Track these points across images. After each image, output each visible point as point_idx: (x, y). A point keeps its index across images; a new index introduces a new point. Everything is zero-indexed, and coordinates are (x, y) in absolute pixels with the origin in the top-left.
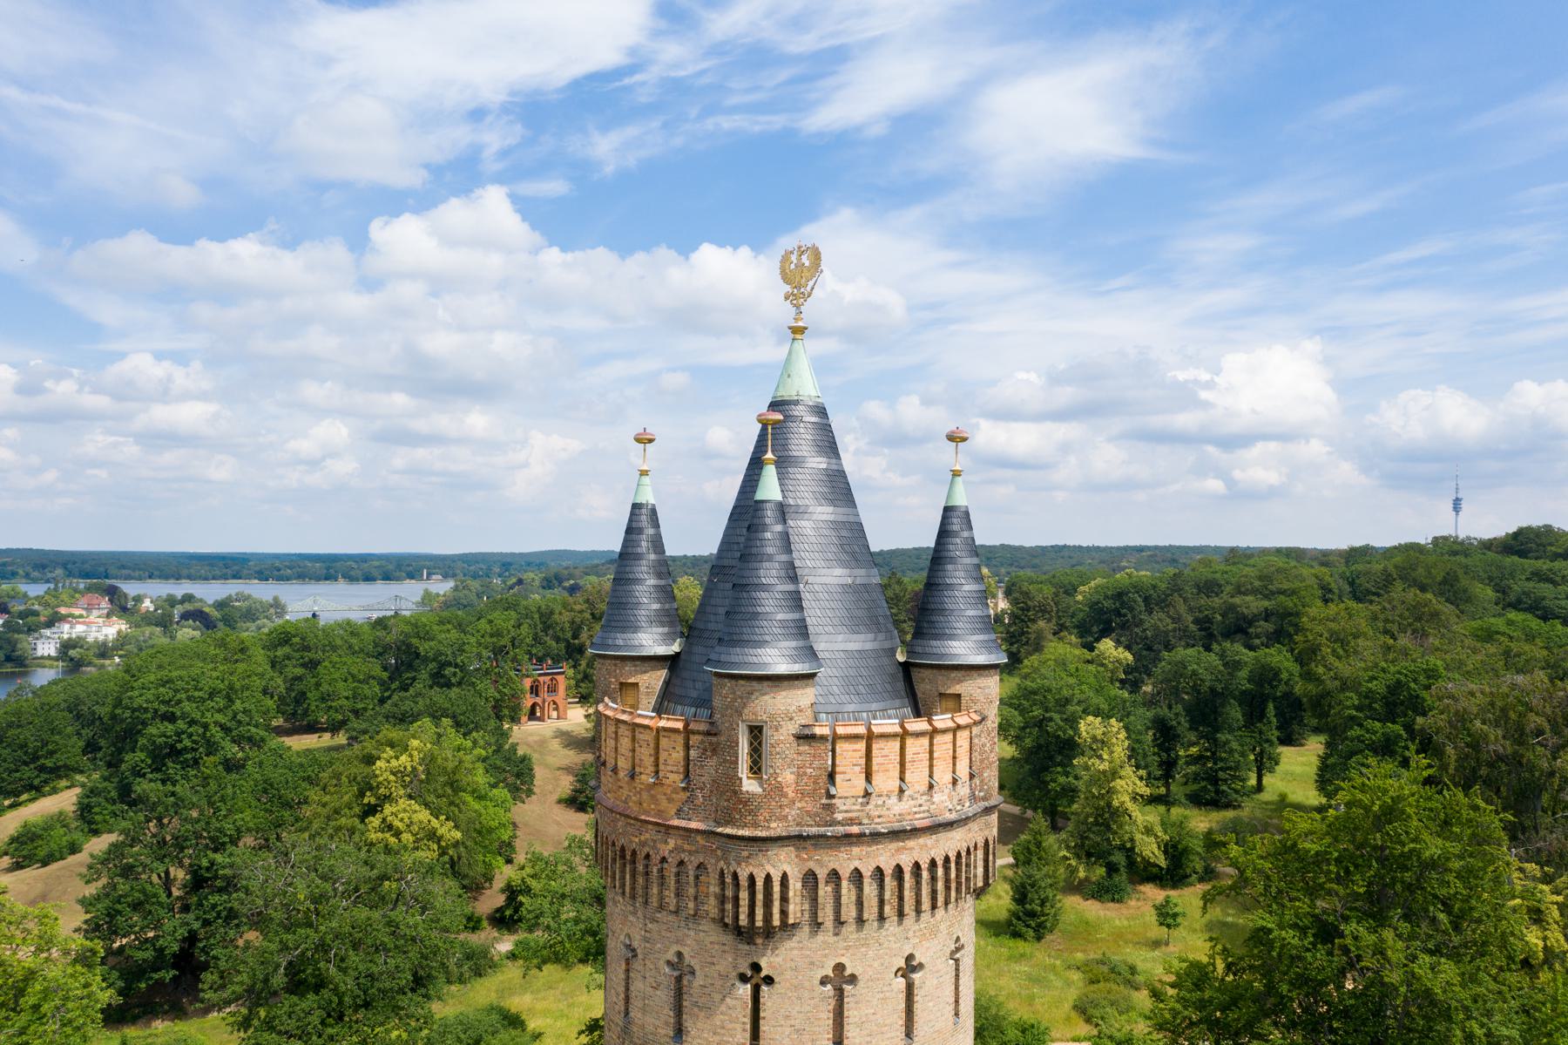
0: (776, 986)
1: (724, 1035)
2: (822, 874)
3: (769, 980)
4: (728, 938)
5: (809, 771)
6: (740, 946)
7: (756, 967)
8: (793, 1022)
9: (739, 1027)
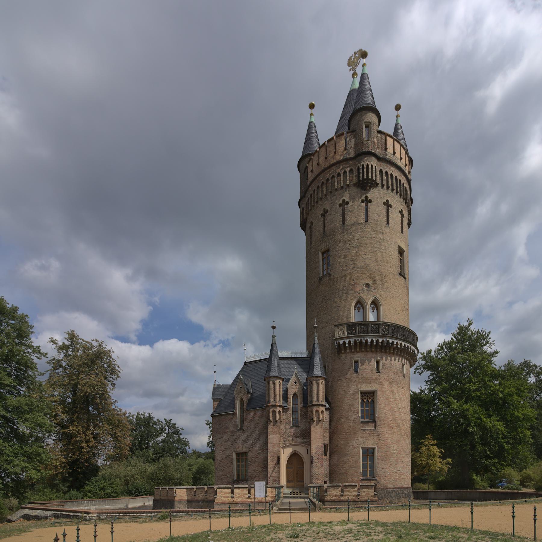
0: (372, 202)
1: (358, 217)
2: (384, 172)
3: (370, 201)
4: (359, 190)
5: (380, 142)
6: (362, 192)
7: (366, 197)
8: (377, 213)
9: (362, 214)
